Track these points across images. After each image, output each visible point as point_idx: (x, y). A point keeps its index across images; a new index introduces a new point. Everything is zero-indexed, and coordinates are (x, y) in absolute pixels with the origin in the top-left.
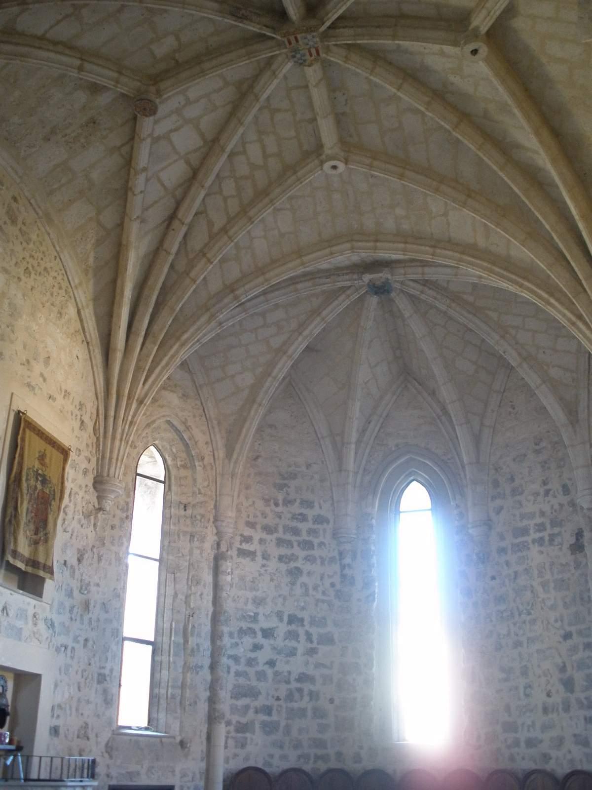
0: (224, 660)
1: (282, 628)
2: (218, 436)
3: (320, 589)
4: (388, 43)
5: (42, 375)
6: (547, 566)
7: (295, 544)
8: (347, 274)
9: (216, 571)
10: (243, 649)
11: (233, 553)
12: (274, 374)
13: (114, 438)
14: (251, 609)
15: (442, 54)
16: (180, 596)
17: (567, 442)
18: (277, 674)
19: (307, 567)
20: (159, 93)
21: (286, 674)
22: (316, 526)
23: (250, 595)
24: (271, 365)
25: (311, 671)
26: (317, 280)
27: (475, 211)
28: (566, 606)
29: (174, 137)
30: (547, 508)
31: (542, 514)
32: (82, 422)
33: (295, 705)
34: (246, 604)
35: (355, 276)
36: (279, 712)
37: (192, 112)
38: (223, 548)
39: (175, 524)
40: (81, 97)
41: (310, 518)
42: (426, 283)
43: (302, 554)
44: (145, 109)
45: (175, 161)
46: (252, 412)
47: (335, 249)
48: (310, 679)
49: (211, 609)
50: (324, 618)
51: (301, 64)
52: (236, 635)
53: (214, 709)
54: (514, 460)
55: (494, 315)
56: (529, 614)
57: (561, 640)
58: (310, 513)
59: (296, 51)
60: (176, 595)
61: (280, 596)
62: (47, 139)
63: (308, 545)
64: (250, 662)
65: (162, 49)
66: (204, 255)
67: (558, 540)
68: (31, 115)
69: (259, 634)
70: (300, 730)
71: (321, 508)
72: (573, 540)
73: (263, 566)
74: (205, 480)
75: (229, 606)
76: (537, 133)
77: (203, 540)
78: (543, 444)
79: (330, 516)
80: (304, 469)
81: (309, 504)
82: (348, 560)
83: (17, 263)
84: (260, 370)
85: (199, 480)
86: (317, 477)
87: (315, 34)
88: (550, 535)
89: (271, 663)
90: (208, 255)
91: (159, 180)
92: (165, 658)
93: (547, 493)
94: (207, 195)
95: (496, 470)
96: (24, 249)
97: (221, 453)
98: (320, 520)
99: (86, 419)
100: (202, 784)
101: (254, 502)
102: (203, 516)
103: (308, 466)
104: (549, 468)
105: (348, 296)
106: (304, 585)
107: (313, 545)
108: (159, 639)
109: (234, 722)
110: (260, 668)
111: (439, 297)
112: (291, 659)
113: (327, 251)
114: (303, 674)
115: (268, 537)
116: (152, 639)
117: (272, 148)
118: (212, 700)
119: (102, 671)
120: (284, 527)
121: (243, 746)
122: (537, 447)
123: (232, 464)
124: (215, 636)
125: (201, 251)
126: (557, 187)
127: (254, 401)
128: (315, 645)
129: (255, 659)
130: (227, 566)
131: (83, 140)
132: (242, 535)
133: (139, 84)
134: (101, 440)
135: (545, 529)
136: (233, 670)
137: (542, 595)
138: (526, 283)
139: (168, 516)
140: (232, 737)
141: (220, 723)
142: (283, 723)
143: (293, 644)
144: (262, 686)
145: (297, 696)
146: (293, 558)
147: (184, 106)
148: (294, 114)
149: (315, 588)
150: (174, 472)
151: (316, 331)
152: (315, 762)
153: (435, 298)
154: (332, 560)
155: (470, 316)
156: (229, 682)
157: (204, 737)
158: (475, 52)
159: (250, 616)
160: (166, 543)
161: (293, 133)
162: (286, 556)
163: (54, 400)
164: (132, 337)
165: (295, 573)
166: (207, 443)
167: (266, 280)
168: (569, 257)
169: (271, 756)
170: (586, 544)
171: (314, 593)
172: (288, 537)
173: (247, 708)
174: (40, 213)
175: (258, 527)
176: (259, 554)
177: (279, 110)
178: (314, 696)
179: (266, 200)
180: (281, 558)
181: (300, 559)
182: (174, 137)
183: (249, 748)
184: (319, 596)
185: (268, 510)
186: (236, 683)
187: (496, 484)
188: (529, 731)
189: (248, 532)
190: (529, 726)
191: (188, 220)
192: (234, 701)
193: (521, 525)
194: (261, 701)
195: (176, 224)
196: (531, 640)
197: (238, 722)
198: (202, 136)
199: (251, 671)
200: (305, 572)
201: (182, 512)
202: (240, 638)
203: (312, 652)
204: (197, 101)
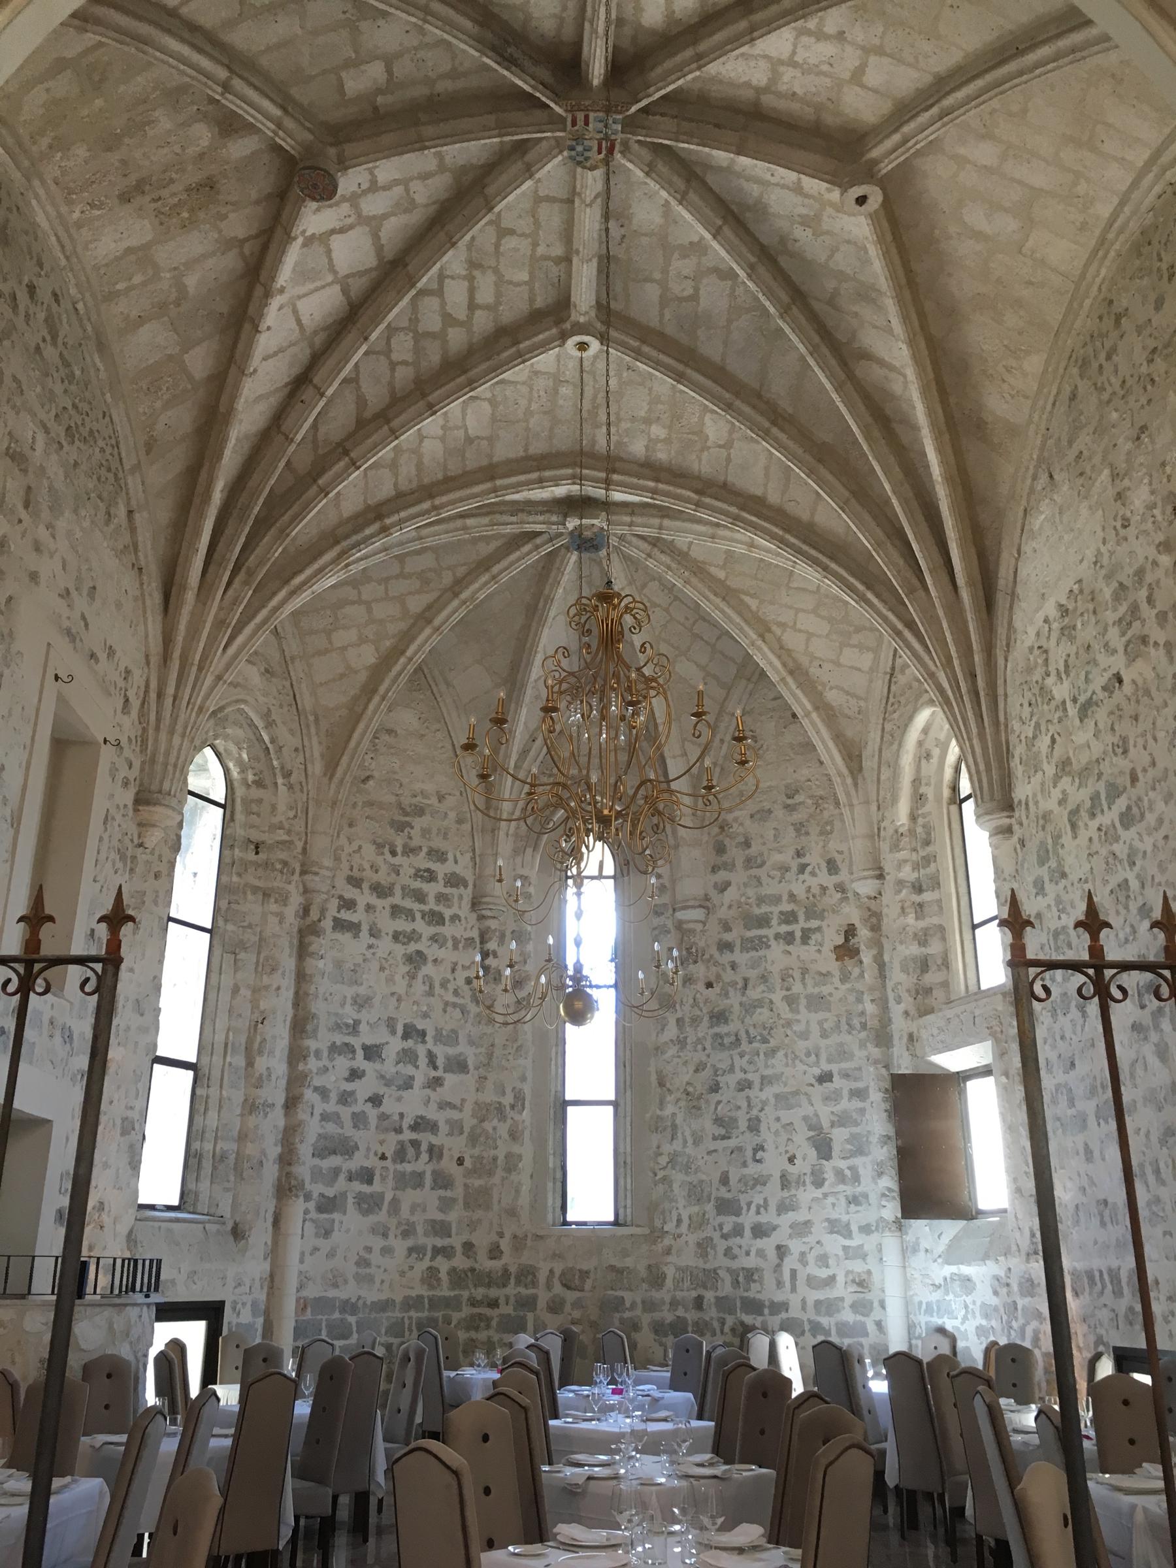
0: (309, 1095)
1: (395, 1045)
2: (315, 740)
3: (451, 987)
4: (721, 157)
5: (83, 618)
6: (797, 974)
7: (418, 916)
8: (542, 513)
9: (302, 951)
10: (334, 1077)
11: (328, 924)
12: (409, 653)
13: (172, 732)
14: (349, 1013)
15: (798, 189)
16: (243, 991)
17: (842, 797)
18: (383, 1117)
19: (432, 952)
20: (344, 164)
21: (396, 1117)
22: (448, 890)
23: (350, 992)
24: (407, 637)
25: (432, 1114)
26: (498, 516)
27: (781, 447)
28: (824, 1035)
29: (336, 242)
30: (799, 890)
31: (792, 897)
32: (127, 700)
33: (408, 1168)
34: (343, 1005)
35: (554, 518)
36: (383, 1178)
37: (374, 205)
38: (314, 915)
39: (239, 875)
40: (203, 134)
41: (440, 876)
42: (655, 542)
43: (426, 930)
44: (315, 186)
45: (329, 285)
46: (371, 707)
47: (547, 474)
48: (433, 1127)
49: (290, 1013)
50: (454, 1031)
51: (579, 163)
52: (325, 1054)
53: (288, 1174)
54: (752, 816)
55: (753, 603)
56: (765, 1041)
57: (813, 1081)
58: (441, 870)
59: (578, 139)
60: (235, 990)
61: (393, 994)
63: (436, 918)
64: (345, 1098)
65: (356, 83)
66: (346, 453)
67: (815, 937)
68: (109, 149)
69: (360, 1053)
70: (413, 1209)
71: (456, 862)
72: (840, 940)
73: (370, 947)
74: (291, 808)
75: (318, 1007)
76: (911, 343)
77: (284, 900)
78: (799, 798)
79: (470, 877)
80: (434, 801)
81: (439, 856)
82: (492, 945)
83: (57, 416)
84: (388, 643)
85: (282, 807)
86: (452, 815)
87: (620, 117)
88: (803, 930)
89: (376, 1100)
90: (352, 455)
91: (295, 312)
92: (214, 1092)
93: (802, 868)
94: (366, 353)
95: (722, 828)
96: (66, 391)
97: (317, 768)
98: (454, 881)
99: (131, 694)
100: (263, 1297)
101: (360, 847)
102: (285, 863)
103: (441, 798)
104: (807, 833)
105: (537, 547)
106: (428, 980)
107: (443, 919)
108: (205, 1060)
109: (315, 1195)
110: (357, 1108)
111: (674, 565)
112: (405, 1094)
113: (534, 476)
114: (422, 1117)
115: (379, 903)
116: (193, 1060)
117: (485, 295)
118: (287, 1158)
119: (130, 1114)
120: (403, 888)
121: (327, 1234)
122: (790, 802)
123: (333, 786)
124: (296, 1055)
125: (339, 444)
126: (915, 428)
127: (374, 691)
128: (439, 1073)
129: (352, 1093)
130: (317, 944)
131: (185, 215)
132: (341, 897)
133: (311, 137)
134: (151, 732)
135: (796, 921)
136: (317, 1112)
137: (786, 1013)
138: (833, 566)
139: (228, 860)
140: (312, 1220)
141: (297, 1196)
142: (388, 1197)
143: (409, 1070)
144: (362, 1138)
145: (411, 1152)
146: (413, 937)
148: (535, 245)
149: (444, 985)
150: (240, 792)
151: (482, 596)
152: (433, 1259)
153: (669, 568)
154: (470, 941)
155: (718, 601)
156: (313, 1129)
157: (270, 1220)
158: (861, 200)
159: (347, 1025)
160: (224, 904)
161: (524, 276)
162: (403, 933)
163: (97, 661)
164: (212, 569)
165: (416, 960)
166: (296, 750)
167: (435, 508)
168: (911, 537)
169: (369, 1249)
170: (862, 947)
171: (442, 992)
172: (408, 903)
173: (336, 1171)
174: (89, 329)
175: (365, 886)
176: (365, 928)
177: (511, 232)
178: (435, 1152)
179: (462, 379)
180: (396, 937)
181: (424, 939)
182: (336, 242)
183: (336, 1235)
184: (451, 998)
185: (379, 860)
186: (321, 1131)
187: (720, 849)
188: (758, 1213)
189: (350, 893)
190: (758, 1207)
191: (330, 392)
192: (317, 1161)
193: (757, 911)
194: (358, 1161)
195: (308, 393)
196: (766, 1081)
197: (322, 1195)
198: (379, 249)
199: (346, 1113)
200: (430, 958)
201: (251, 856)
202: (332, 1060)
203: (436, 1082)
204: (387, 188)
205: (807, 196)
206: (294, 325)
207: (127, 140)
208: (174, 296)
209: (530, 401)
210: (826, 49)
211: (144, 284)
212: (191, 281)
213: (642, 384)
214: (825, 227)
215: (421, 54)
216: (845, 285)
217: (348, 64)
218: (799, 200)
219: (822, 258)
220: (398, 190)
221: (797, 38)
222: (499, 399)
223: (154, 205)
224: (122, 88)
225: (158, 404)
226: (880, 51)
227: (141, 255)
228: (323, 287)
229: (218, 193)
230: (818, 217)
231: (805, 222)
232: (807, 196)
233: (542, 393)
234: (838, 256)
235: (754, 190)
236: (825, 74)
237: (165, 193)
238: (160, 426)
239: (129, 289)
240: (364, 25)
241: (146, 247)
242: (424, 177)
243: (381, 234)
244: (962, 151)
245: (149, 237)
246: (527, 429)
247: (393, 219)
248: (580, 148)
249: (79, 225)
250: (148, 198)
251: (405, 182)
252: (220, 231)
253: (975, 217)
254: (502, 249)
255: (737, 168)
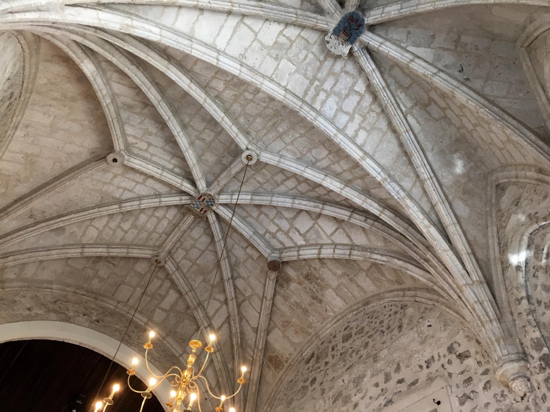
29: (303, 231)
37: (285, 225)
40: (293, 286)
62: (320, 301)
68: (307, 311)
91: (332, 234)
131: (319, 281)
147: (282, 231)
177: (258, 182)
182: (303, 231)
204: (278, 226)
205: (147, 142)
206: (337, 232)
207: (303, 307)
208: (347, 277)
209: (296, 139)
210: (123, 185)
211: (346, 287)
212: (339, 272)
213: (245, 113)
214: (142, 131)
215: (237, 242)
216: (138, 111)
217: (252, 259)
218: (150, 141)
219: (147, 121)
220: (276, 221)
221: (133, 189)
222: (307, 149)
223: (320, 292)
224: (288, 314)
225: (383, 278)
226: (105, 183)
227: (336, 290)
228: (320, 226)
229: (308, 273)
230: (144, 134)
231: (151, 134)
232: (147, 142)
233: (290, 136)
234: (139, 121)
235: (167, 148)
236: (127, 178)
237: (314, 290)
238: (391, 278)
239: (351, 292)
240: (242, 261)
241: (335, 290)
242: (267, 216)
243: (293, 216)
244: (81, 149)
245: (331, 290)
246: (307, 132)
247: (286, 216)
248: (210, 203)
249: (334, 312)
250: (318, 294)
251: (272, 221)
252: (320, 268)
253: (76, 128)
254: (265, 181)
255: (172, 156)
